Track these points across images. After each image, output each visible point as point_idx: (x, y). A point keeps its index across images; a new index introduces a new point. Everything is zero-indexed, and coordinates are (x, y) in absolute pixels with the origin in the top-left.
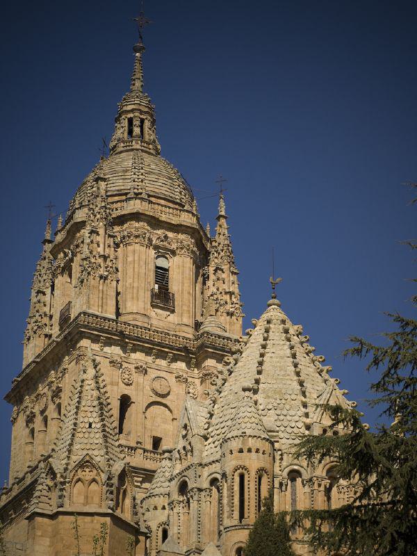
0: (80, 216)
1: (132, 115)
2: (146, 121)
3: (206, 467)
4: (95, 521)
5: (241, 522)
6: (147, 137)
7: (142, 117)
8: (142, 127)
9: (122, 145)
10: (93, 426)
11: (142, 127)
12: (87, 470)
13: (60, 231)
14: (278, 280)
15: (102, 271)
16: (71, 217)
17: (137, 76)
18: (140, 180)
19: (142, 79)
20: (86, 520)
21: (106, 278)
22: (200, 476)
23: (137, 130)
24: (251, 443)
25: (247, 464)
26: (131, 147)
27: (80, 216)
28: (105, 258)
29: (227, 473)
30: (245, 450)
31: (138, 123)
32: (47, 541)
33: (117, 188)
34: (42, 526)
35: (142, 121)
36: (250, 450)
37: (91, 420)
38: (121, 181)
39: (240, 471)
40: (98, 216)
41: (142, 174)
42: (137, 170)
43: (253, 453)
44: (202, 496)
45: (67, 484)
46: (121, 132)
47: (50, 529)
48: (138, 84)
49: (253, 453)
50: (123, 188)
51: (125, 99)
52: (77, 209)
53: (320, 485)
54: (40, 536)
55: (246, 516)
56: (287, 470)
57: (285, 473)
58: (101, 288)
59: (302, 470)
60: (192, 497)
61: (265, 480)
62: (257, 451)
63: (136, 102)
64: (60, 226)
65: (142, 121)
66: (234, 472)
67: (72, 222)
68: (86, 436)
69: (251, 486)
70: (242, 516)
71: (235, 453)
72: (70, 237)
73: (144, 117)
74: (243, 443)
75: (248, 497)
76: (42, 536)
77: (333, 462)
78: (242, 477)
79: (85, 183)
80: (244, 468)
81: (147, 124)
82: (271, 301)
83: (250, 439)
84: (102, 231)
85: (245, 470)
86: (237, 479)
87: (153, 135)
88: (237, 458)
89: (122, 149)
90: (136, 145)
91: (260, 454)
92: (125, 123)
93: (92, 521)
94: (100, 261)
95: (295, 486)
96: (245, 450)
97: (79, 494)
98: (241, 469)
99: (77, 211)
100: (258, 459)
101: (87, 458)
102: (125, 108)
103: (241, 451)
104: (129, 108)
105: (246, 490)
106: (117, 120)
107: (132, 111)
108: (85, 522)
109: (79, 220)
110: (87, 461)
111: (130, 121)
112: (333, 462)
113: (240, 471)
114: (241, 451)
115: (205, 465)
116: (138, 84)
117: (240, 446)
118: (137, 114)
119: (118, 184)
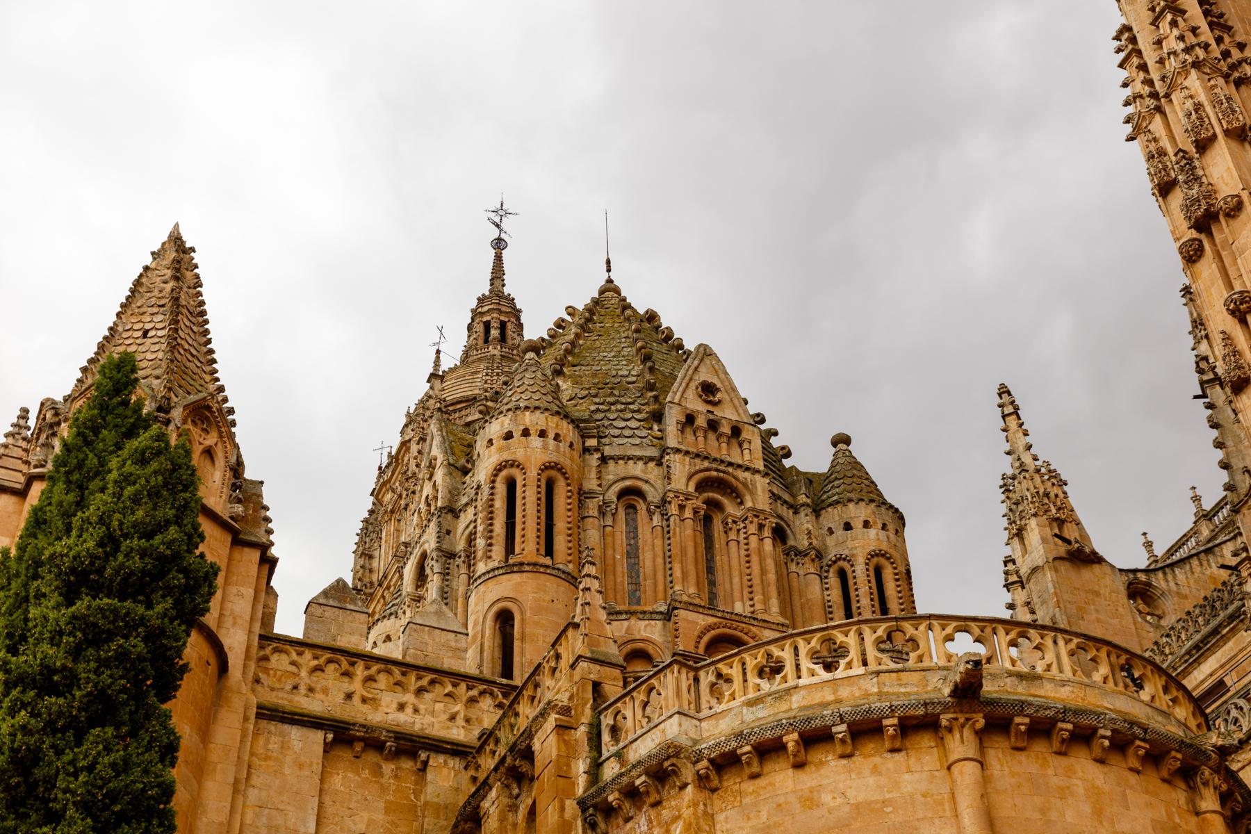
1: (489, 318)
5: (507, 560)
7: (502, 318)
30: (517, 434)
36: (526, 433)
38: (467, 385)
41: (498, 374)
53: (682, 508)
55: (517, 550)
57: (612, 495)
59: (645, 487)
61: (561, 489)
62: (543, 434)
66: (496, 475)
70: (510, 548)
73: (506, 320)
74: (513, 420)
78: (511, 485)
80: (513, 464)
86: (501, 488)
95: (635, 520)
100: (545, 447)
103: (509, 436)
105: (519, 502)
113: (504, 473)
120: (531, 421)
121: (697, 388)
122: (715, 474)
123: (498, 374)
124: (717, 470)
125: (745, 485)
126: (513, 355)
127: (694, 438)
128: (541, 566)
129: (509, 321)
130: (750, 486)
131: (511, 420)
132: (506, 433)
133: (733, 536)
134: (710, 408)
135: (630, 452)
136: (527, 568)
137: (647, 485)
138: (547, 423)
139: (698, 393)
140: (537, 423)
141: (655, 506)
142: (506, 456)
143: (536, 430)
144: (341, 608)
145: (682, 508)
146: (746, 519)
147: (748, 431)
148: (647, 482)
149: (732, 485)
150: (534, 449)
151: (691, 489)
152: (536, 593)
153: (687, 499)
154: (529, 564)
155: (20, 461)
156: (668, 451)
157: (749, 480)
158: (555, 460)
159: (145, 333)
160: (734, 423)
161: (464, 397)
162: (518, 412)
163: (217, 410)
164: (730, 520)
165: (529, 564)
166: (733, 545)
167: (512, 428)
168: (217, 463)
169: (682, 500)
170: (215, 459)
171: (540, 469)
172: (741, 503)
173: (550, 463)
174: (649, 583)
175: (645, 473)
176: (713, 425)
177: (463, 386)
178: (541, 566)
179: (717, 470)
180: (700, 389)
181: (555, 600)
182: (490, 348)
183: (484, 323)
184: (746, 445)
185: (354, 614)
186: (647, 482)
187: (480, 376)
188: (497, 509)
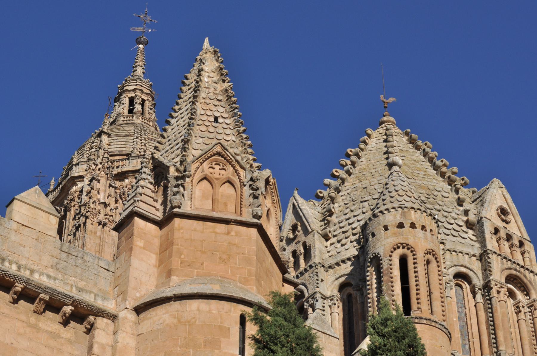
0: (76, 172)
1: (133, 95)
2: (147, 102)
3: (331, 271)
4: (233, 233)
6: (147, 116)
7: (143, 97)
8: (143, 105)
9: (122, 119)
10: (220, 120)
11: (143, 105)
12: (217, 167)
13: (51, 192)
14: (391, 100)
15: (101, 217)
16: (67, 175)
17: (140, 64)
18: (143, 144)
19: (143, 67)
20: (218, 230)
21: (104, 225)
22: (322, 281)
23: (138, 107)
24: (414, 216)
25: (411, 242)
26: (131, 122)
27: (76, 172)
28: (106, 205)
29: (382, 254)
30: (407, 225)
31: (139, 101)
32: (153, 259)
33: (118, 149)
34: (145, 234)
35: (143, 101)
37: (217, 114)
38: (123, 143)
39: (400, 251)
40: (100, 166)
41: (145, 139)
42: (139, 140)
43: (418, 230)
44: (326, 306)
45: (187, 179)
46: (123, 108)
47: (157, 242)
48: (139, 71)
49: (418, 230)
50: (124, 149)
51: (126, 80)
52: (76, 165)
54: (141, 248)
56: (452, 271)
58: (99, 234)
59: (471, 274)
60: (312, 306)
62: (423, 228)
63: (138, 83)
64: (52, 187)
65: (143, 101)
67: (69, 177)
68: (211, 129)
69: (418, 269)
71: (393, 229)
72: (64, 195)
73: (146, 99)
74: (403, 215)
75: (415, 283)
76: (144, 248)
77: (510, 269)
78: (403, 261)
79: (83, 147)
81: (148, 104)
82: (385, 118)
83: (413, 212)
84: (103, 180)
85: (412, 252)
87: (154, 114)
88: (395, 235)
89: (123, 122)
90: (137, 120)
91: (428, 233)
92: (126, 101)
93: (228, 233)
94: (101, 207)
96: (407, 225)
97: (204, 196)
98: (405, 249)
99: (74, 167)
100: (426, 238)
101: (218, 149)
102: (125, 88)
103: (401, 226)
104: (130, 88)
106: (117, 99)
107: (134, 90)
108: (216, 233)
109: (76, 175)
110: (219, 154)
111: (132, 101)
112: (510, 269)
113: (400, 251)
114: (401, 226)
115: (330, 267)
116: (139, 71)
117: (399, 219)
118: (138, 93)
119: (119, 146)
120: (415, 218)
121: (497, 210)
122: (514, 272)
123: (145, 139)
124: (516, 270)
125: (530, 282)
126: (150, 126)
127: (497, 244)
128: (433, 321)
129: (147, 100)
130: (533, 284)
131: (401, 215)
132: (399, 223)
133: (522, 316)
134: (504, 224)
135: (459, 248)
136: (425, 321)
137: (472, 272)
138: (425, 222)
139: (498, 214)
140: (419, 220)
141: (479, 289)
142: (401, 240)
143: (420, 225)
144: (323, 333)
145: (498, 292)
146: (532, 306)
147: (527, 245)
148: (471, 270)
149: (523, 282)
150: (419, 238)
151: (503, 281)
152: (432, 340)
153: (502, 287)
154: (426, 319)
155: (152, 199)
156: (489, 252)
157: (533, 280)
158: (432, 249)
159: (216, 120)
160: (520, 239)
161: (119, 151)
162: (406, 210)
163: (272, 183)
164: (521, 305)
165: (426, 319)
166: (522, 322)
167: (402, 220)
168: (271, 221)
169: (499, 288)
170: (270, 218)
171: (425, 253)
172: (528, 294)
173: (429, 249)
174: (477, 341)
175: (470, 264)
176: (509, 237)
177: (118, 143)
178: (433, 321)
179: (516, 270)
180: (499, 211)
181: (442, 347)
182: (134, 118)
183: (129, 98)
184: (526, 255)
185: (331, 338)
186: (471, 270)
187: (133, 138)
188: (396, 276)
